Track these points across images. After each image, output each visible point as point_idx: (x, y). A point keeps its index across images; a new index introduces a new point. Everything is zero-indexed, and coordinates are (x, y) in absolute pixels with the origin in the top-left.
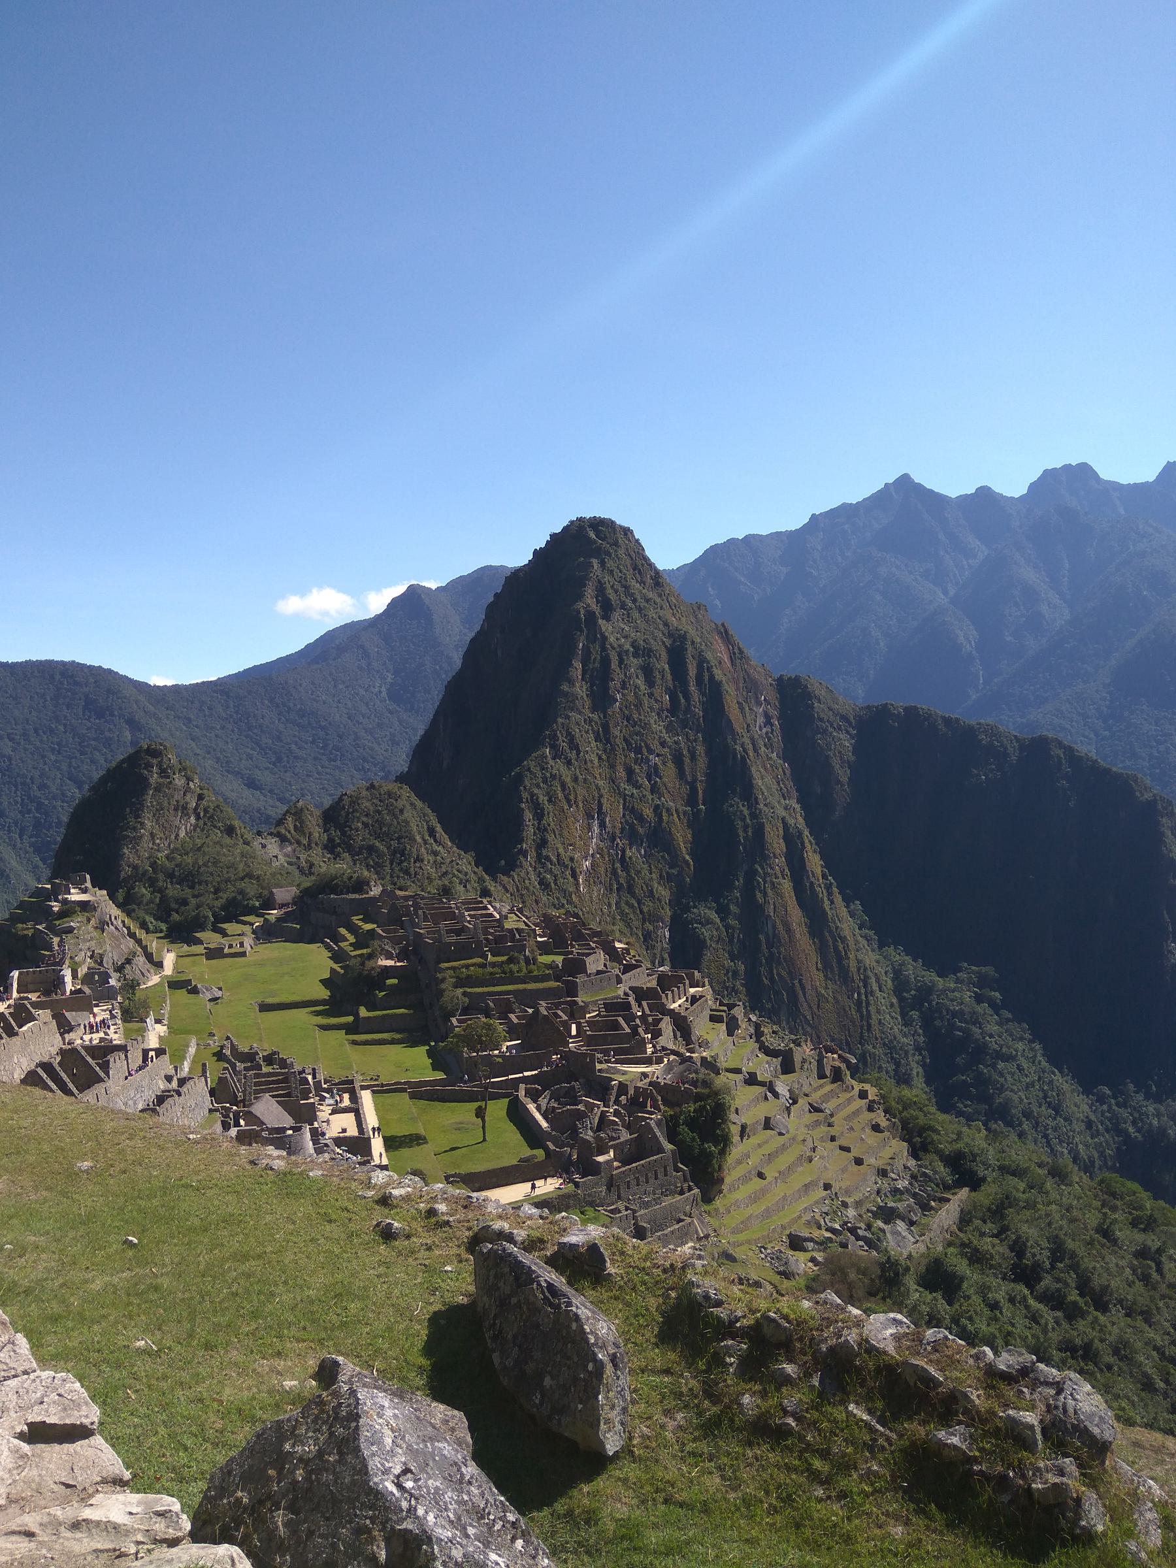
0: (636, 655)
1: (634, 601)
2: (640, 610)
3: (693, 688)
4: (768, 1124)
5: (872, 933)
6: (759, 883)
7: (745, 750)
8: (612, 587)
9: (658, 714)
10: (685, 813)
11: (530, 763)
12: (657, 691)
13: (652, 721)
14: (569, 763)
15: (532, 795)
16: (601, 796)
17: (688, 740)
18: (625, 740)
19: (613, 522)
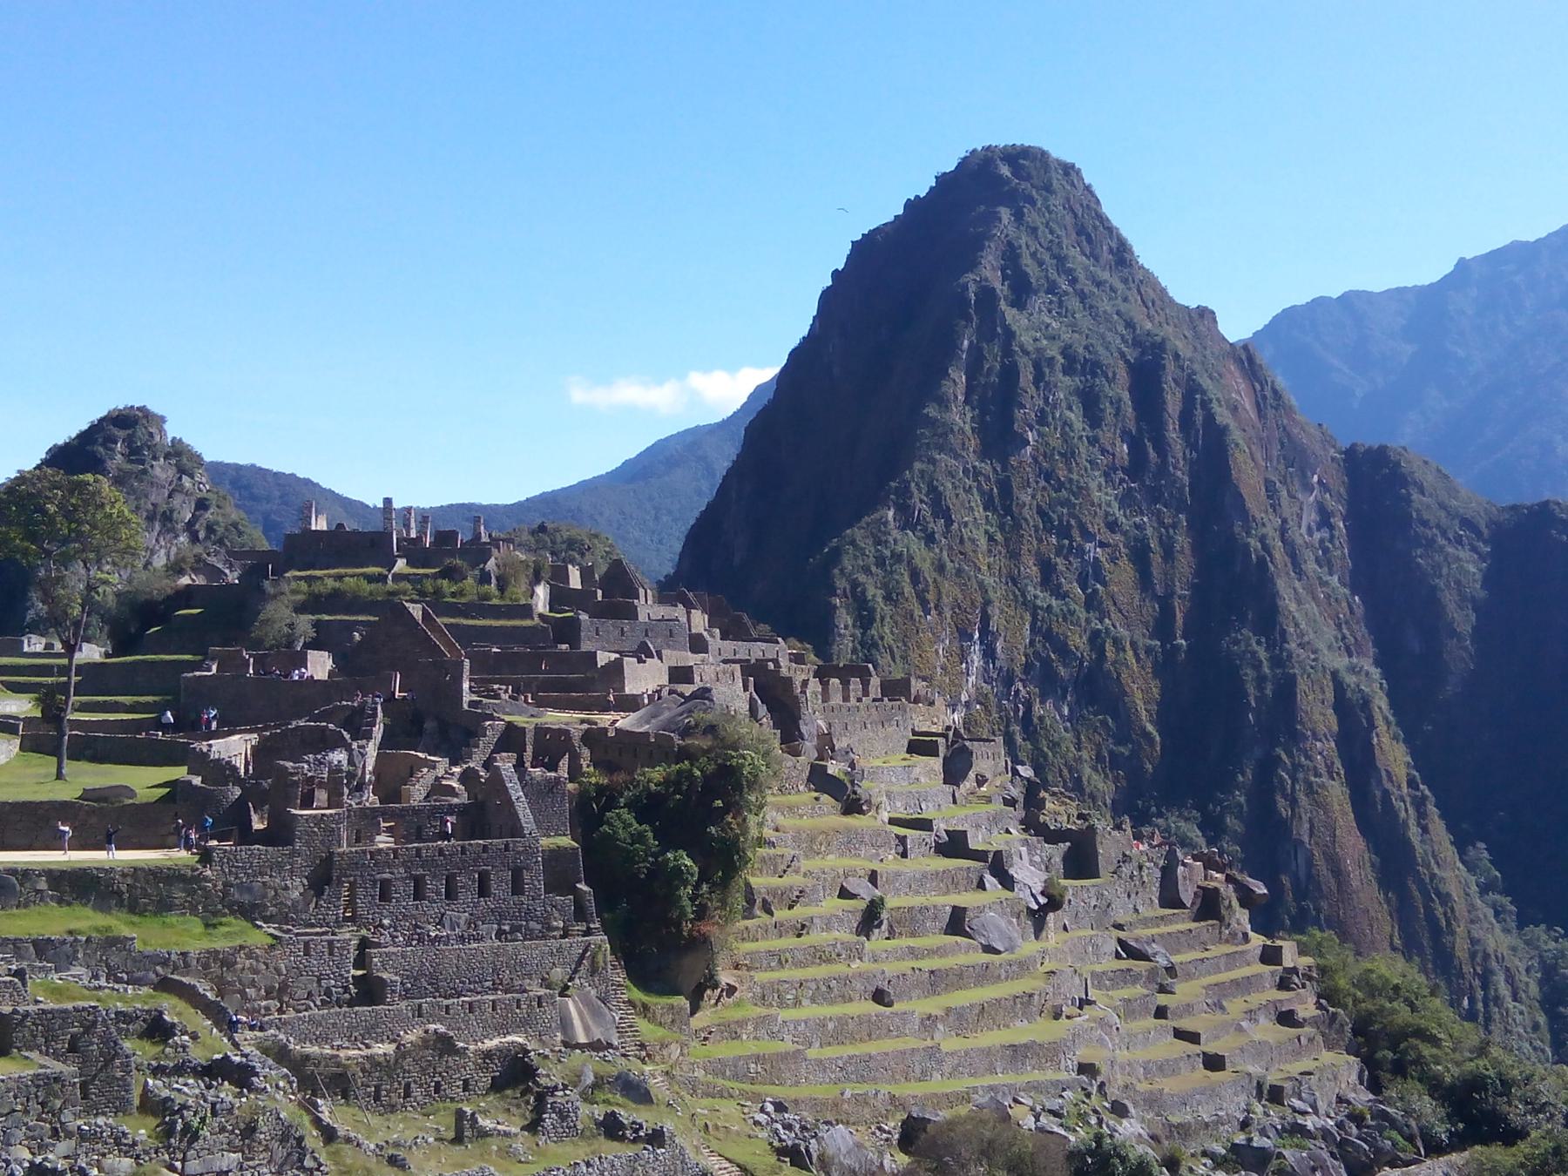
0: (1068, 370)
1: (1073, 281)
2: (1082, 296)
3: (1173, 434)
4: (957, 922)
5: (1506, 900)
6: (1282, 780)
7: (1265, 547)
8: (1034, 255)
9: (1106, 475)
10: (1149, 650)
11: (857, 533)
12: (1106, 435)
13: (1093, 485)
14: (930, 539)
15: (855, 584)
16: (987, 602)
17: (1161, 523)
18: (1041, 512)
19: (1044, 154)
